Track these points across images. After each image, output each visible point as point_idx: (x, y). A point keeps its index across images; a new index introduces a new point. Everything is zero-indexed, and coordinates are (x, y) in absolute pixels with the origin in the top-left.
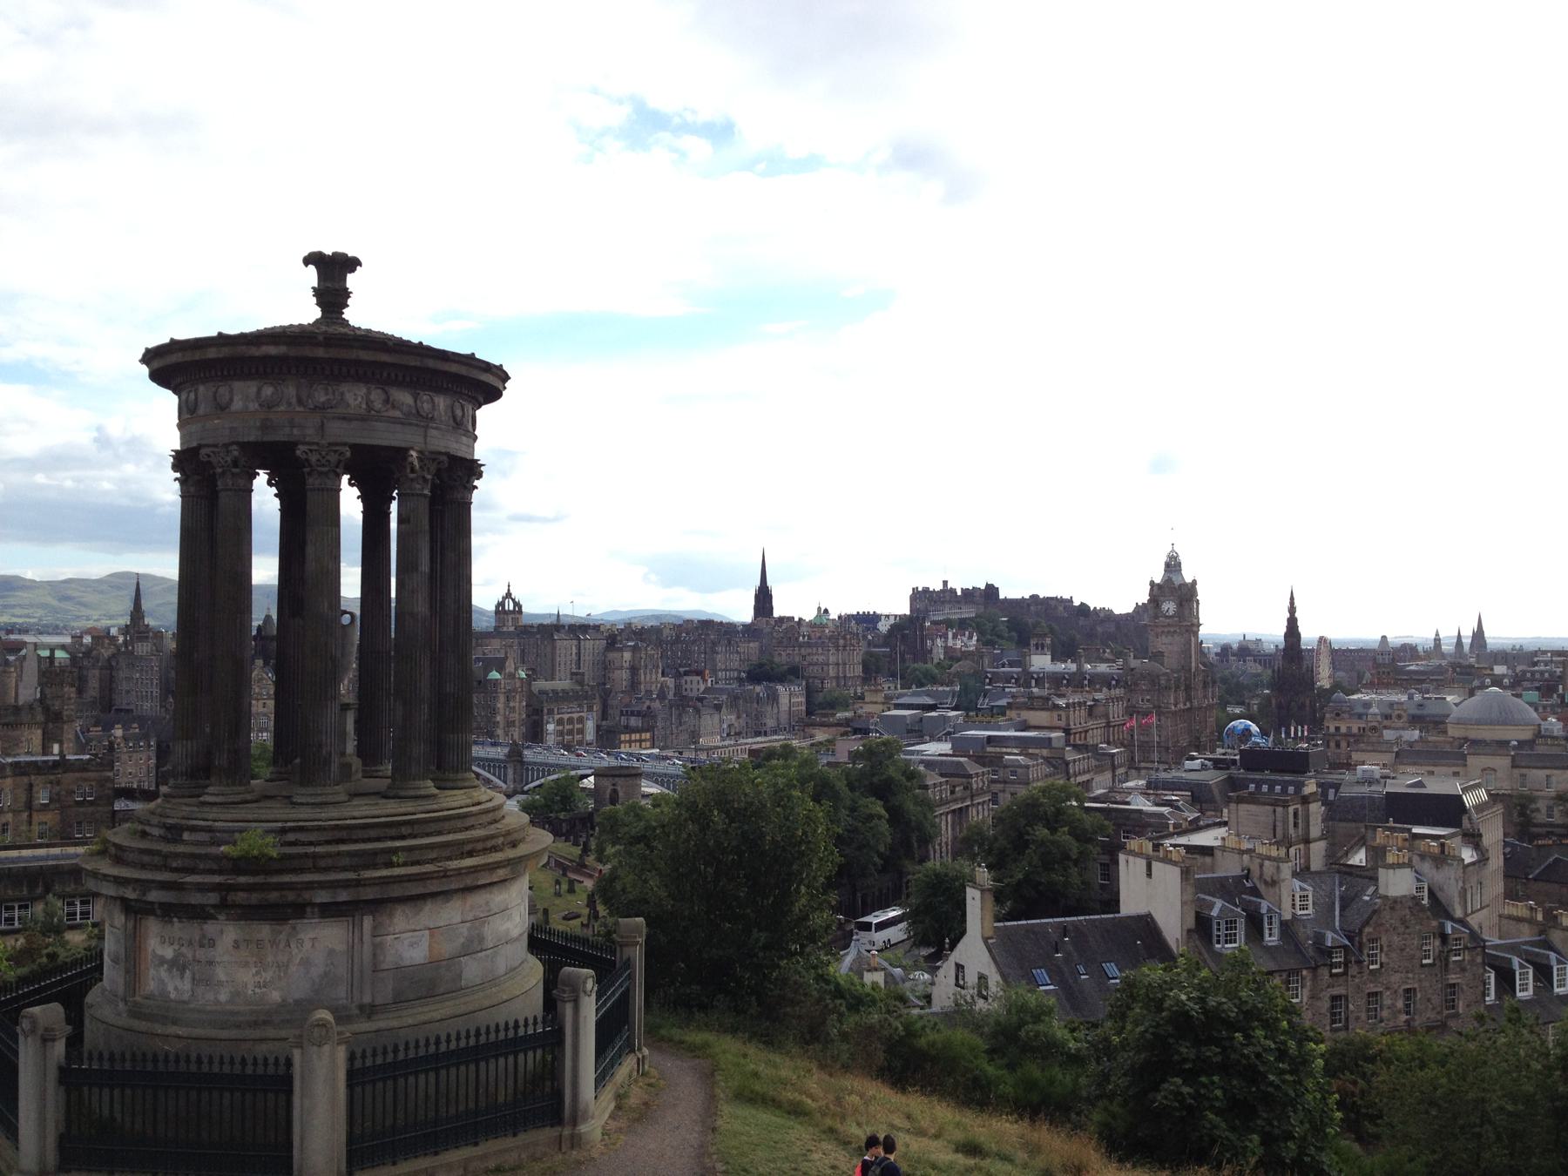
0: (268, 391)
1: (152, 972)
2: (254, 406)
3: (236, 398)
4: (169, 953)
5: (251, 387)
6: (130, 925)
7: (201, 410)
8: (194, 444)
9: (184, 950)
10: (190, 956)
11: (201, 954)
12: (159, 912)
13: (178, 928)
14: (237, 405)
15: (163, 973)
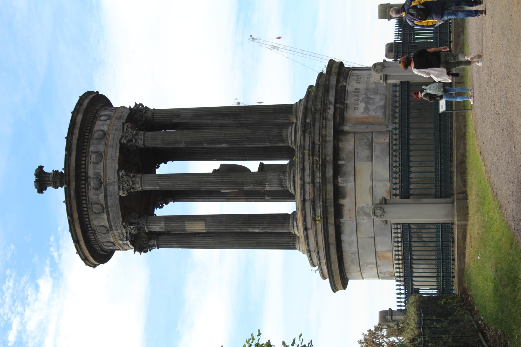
0: (103, 118)
1: (372, 113)
2: (108, 122)
3: (102, 128)
4: (362, 106)
5: (98, 123)
6: (350, 125)
7: (101, 148)
8: (118, 154)
9: (361, 98)
10: (364, 96)
11: (362, 92)
12: (341, 106)
13: (350, 100)
14: (105, 128)
15: (371, 107)
